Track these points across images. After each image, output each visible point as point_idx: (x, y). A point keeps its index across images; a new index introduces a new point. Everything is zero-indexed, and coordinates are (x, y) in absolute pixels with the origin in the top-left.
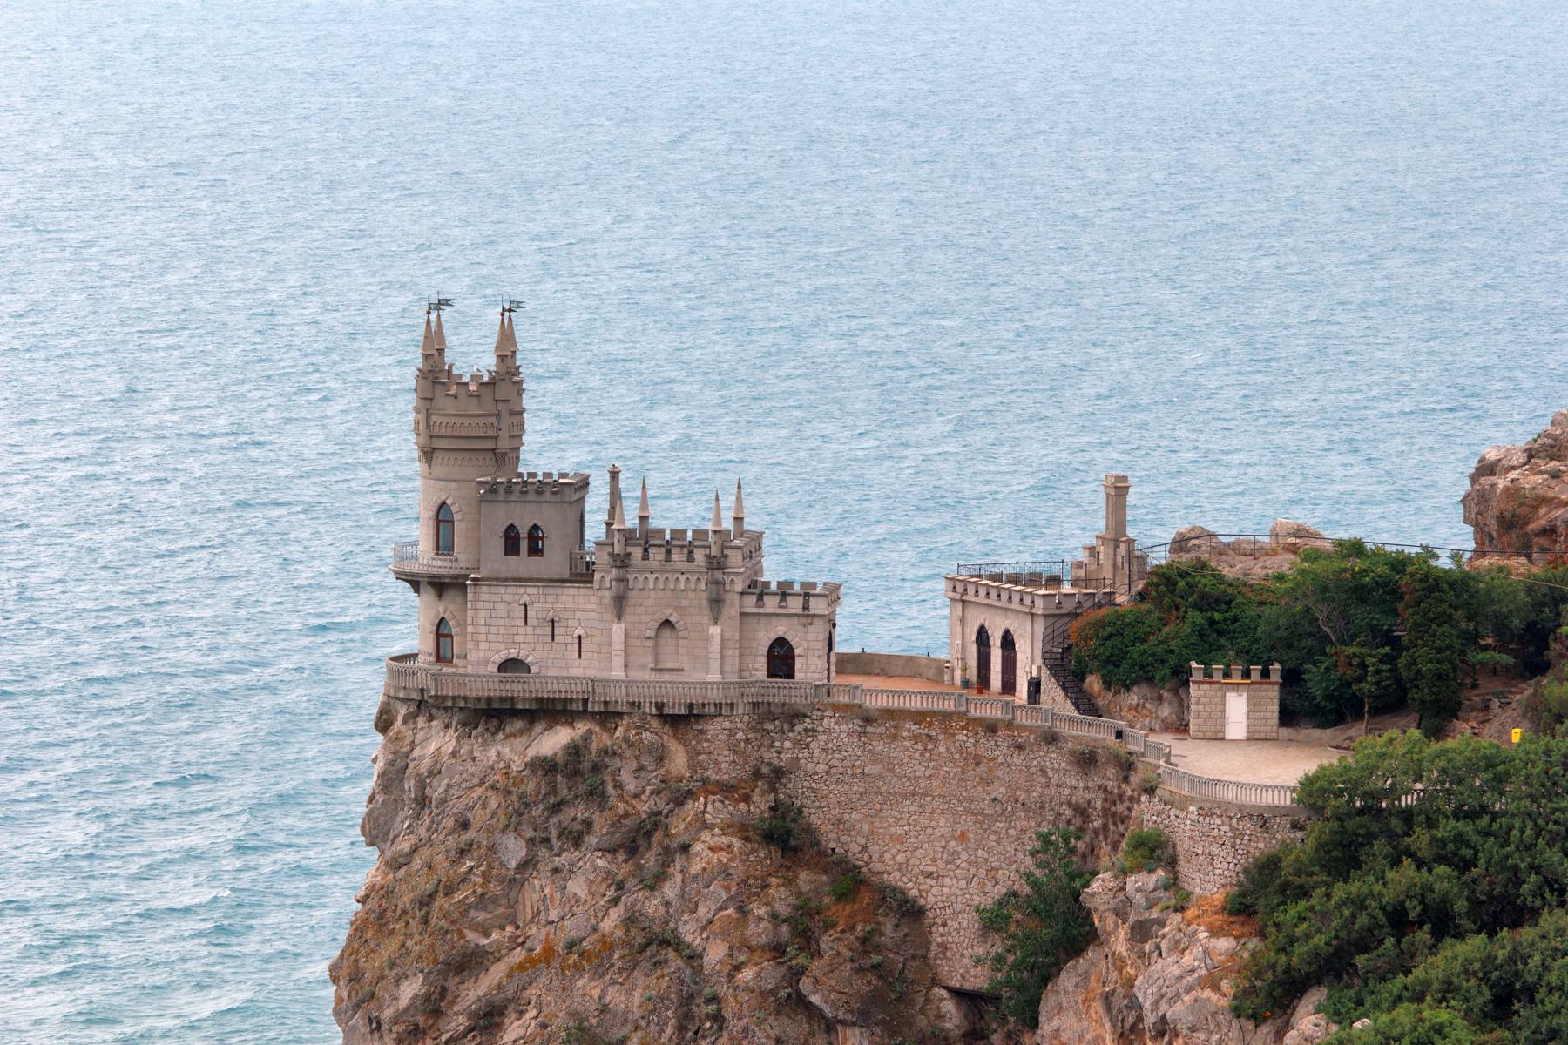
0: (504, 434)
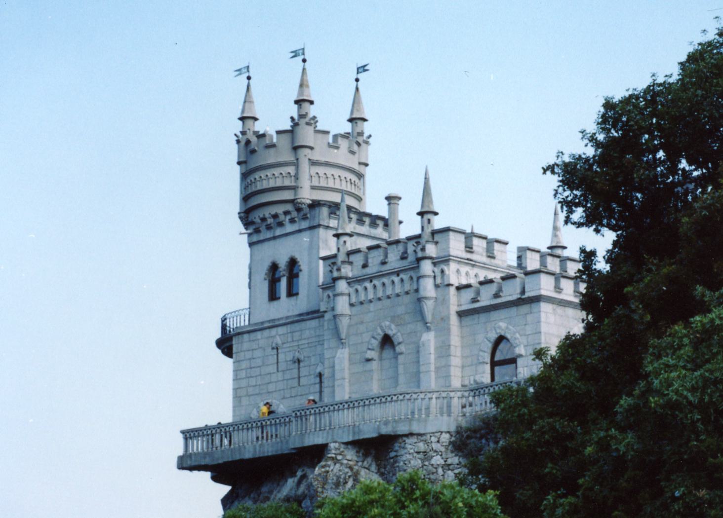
0: (305, 183)
